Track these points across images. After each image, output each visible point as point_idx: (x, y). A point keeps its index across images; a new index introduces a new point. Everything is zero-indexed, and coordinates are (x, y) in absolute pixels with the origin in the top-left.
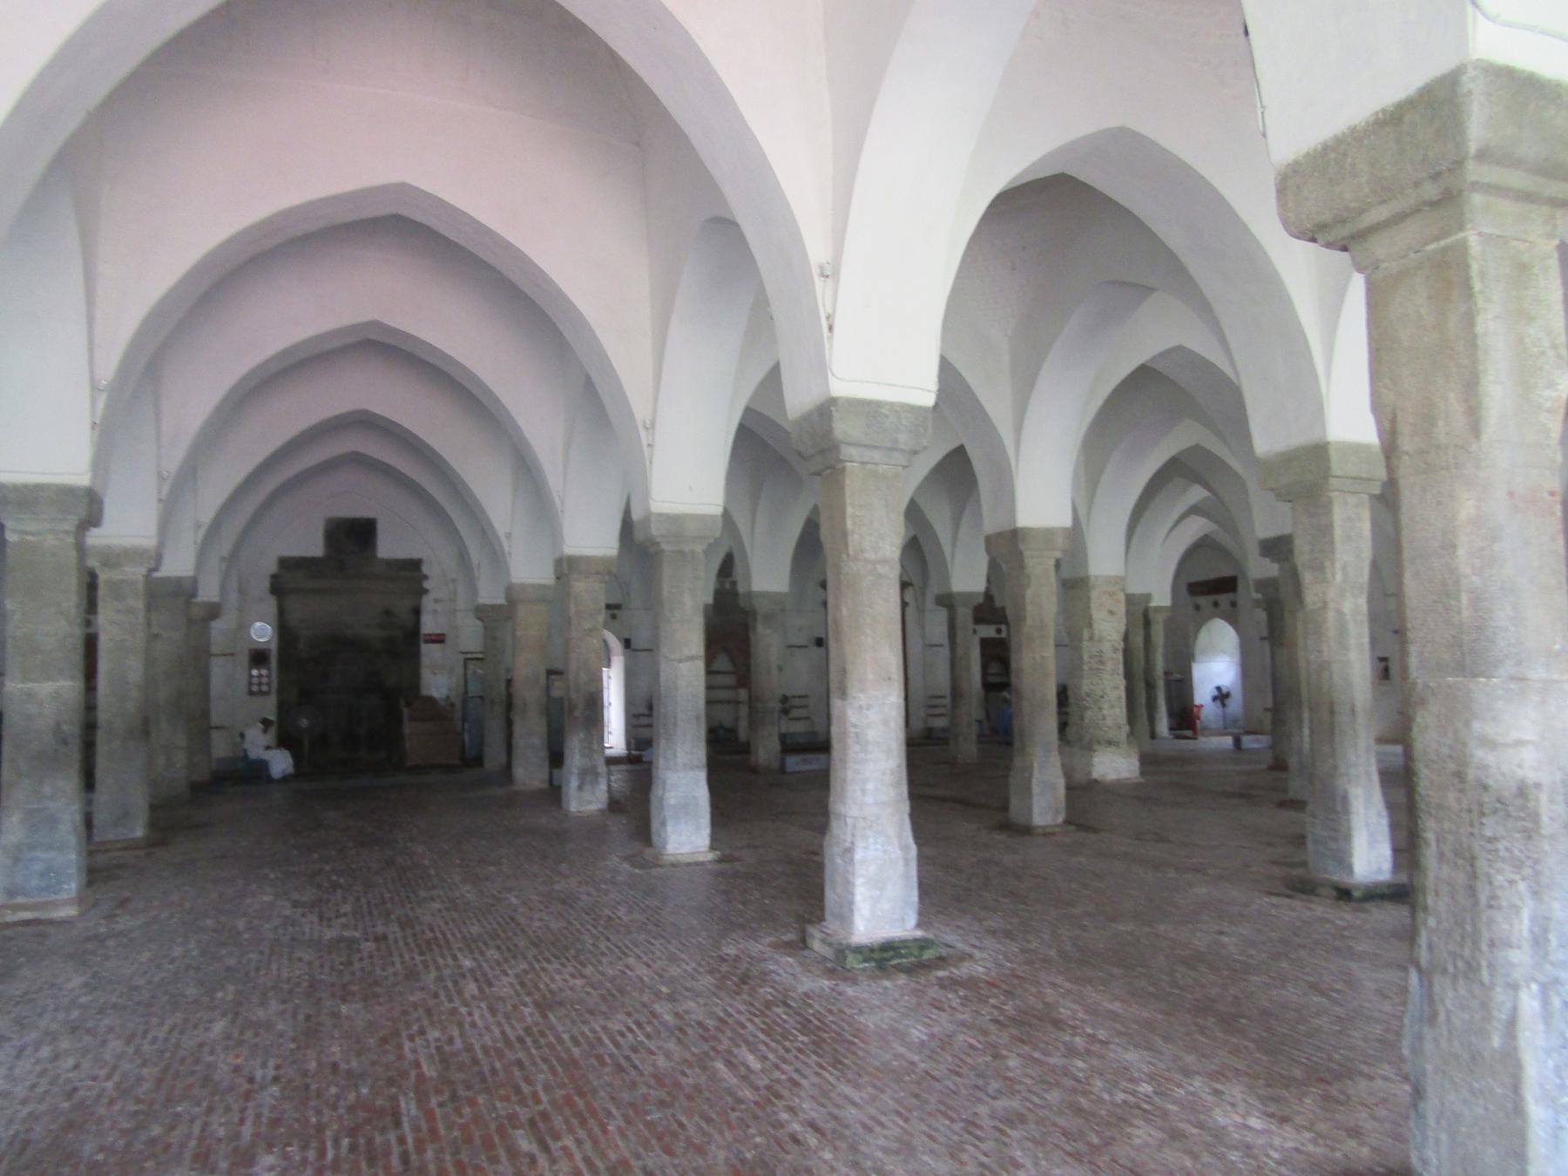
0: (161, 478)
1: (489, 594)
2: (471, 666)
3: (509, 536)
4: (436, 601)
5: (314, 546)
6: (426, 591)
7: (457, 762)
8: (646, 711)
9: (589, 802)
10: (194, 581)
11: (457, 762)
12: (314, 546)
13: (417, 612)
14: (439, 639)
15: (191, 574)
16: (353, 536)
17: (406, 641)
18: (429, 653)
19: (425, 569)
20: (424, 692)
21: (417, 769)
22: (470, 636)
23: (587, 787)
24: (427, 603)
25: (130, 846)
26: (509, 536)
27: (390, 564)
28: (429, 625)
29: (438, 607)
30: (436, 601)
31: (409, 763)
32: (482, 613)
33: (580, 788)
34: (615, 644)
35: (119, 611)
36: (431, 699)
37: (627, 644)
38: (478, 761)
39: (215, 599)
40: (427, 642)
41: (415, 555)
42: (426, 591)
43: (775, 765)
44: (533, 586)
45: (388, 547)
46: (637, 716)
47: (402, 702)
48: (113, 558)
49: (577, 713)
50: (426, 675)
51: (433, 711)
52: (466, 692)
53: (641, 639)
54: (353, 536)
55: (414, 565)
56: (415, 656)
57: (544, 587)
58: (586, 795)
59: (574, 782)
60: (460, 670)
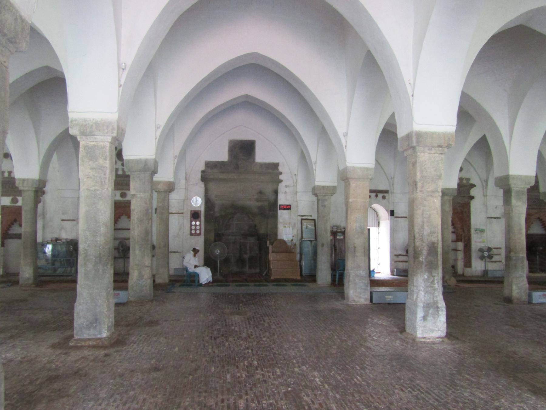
0: (121, 68)
1: (324, 177)
2: (305, 223)
3: (346, 135)
4: (286, 186)
5: (223, 156)
6: (281, 181)
7: (299, 278)
8: (404, 253)
9: (432, 331)
10: (156, 163)
11: (299, 278)
12: (223, 156)
13: (276, 192)
14: (287, 208)
15: (153, 157)
16: (244, 149)
17: (270, 209)
18: (282, 215)
19: (280, 169)
20: (279, 237)
21: (279, 282)
22: (304, 204)
23: (430, 318)
24: (282, 188)
25: (99, 345)
26: (346, 135)
27: (262, 165)
28: (282, 200)
29: (287, 190)
30: (286, 186)
31: (272, 278)
32: (316, 191)
33: (425, 318)
34: (383, 213)
35: (93, 169)
36: (283, 242)
37: (392, 213)
38: (312, 278)
39: (172, 180)
40: (280, 209)
41: (276, 161)
42: (281, 181)
43: (525, 298)
44: (361, 168)
45: (262, 156)
46: (397, 256)
47: (268, 242)
48: (89, 129)
49: (422, 258)
50: (280, 227)
51: (285, 248)
52: (302, 238)
53: (402, 209)
54: (244, 149)
55: (275, 166)
56: (275, 217)
57: (367, 169)
58: (429, 324)
59: (420, 314)
60: (299, 225)
